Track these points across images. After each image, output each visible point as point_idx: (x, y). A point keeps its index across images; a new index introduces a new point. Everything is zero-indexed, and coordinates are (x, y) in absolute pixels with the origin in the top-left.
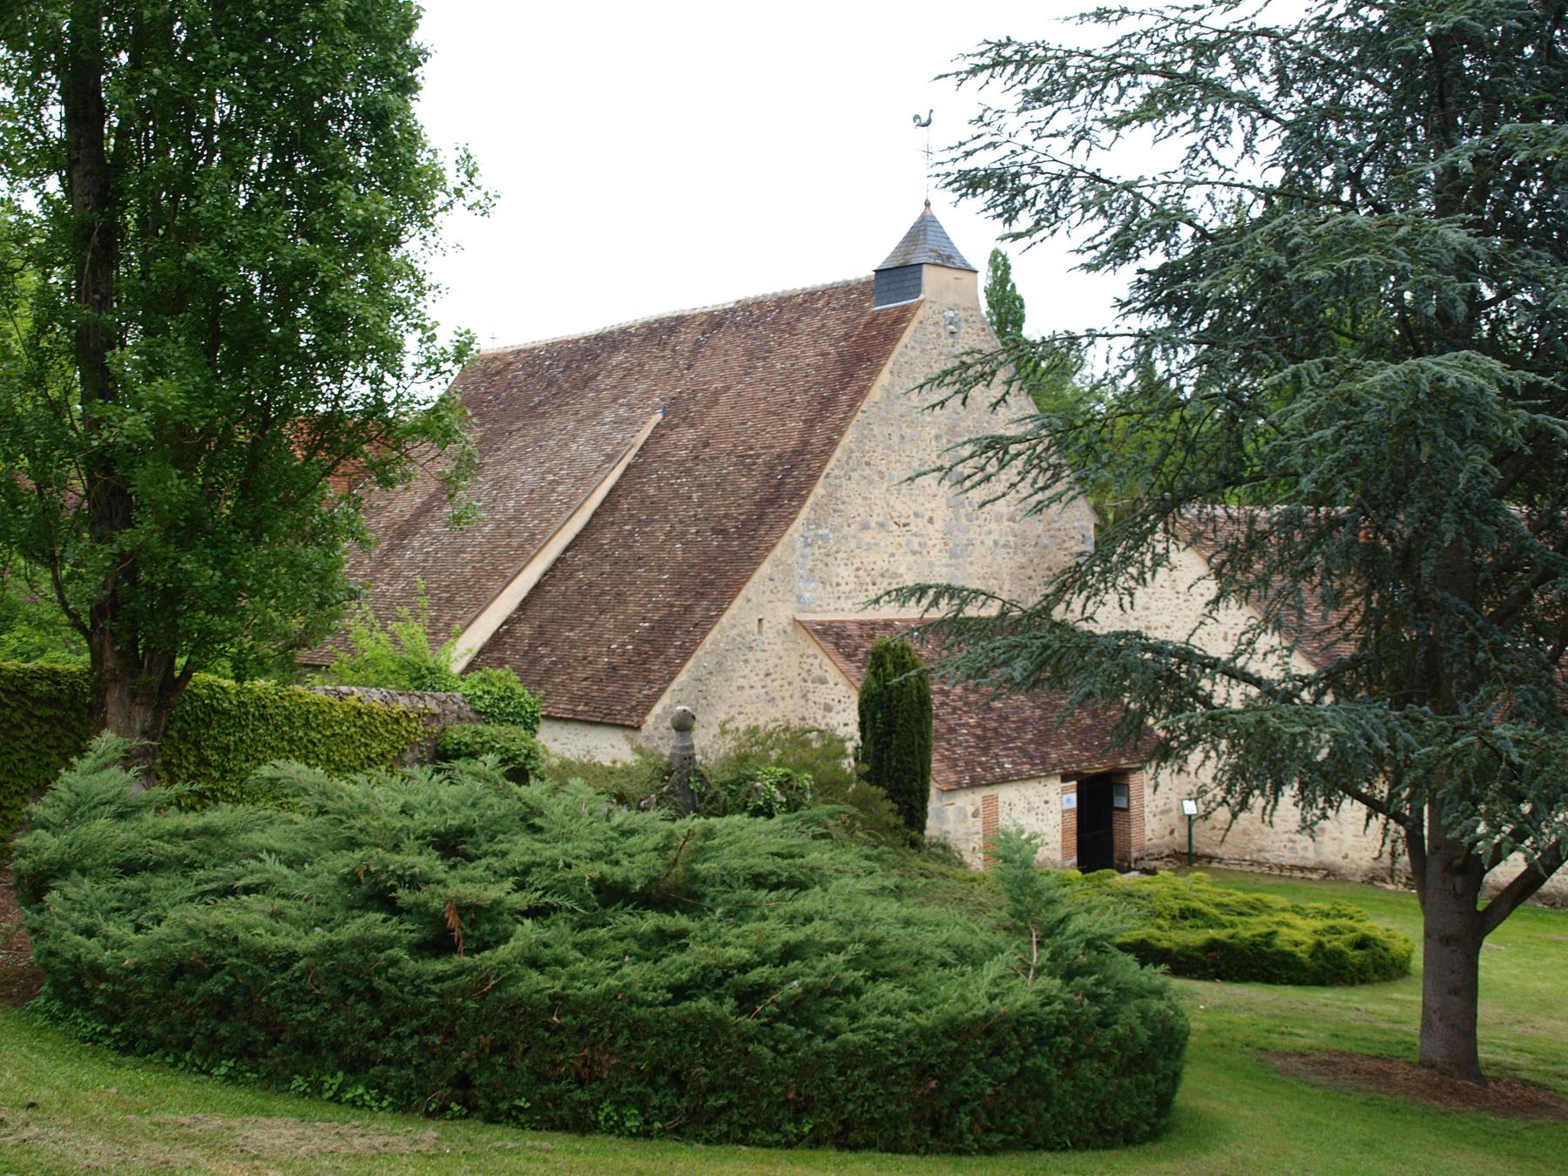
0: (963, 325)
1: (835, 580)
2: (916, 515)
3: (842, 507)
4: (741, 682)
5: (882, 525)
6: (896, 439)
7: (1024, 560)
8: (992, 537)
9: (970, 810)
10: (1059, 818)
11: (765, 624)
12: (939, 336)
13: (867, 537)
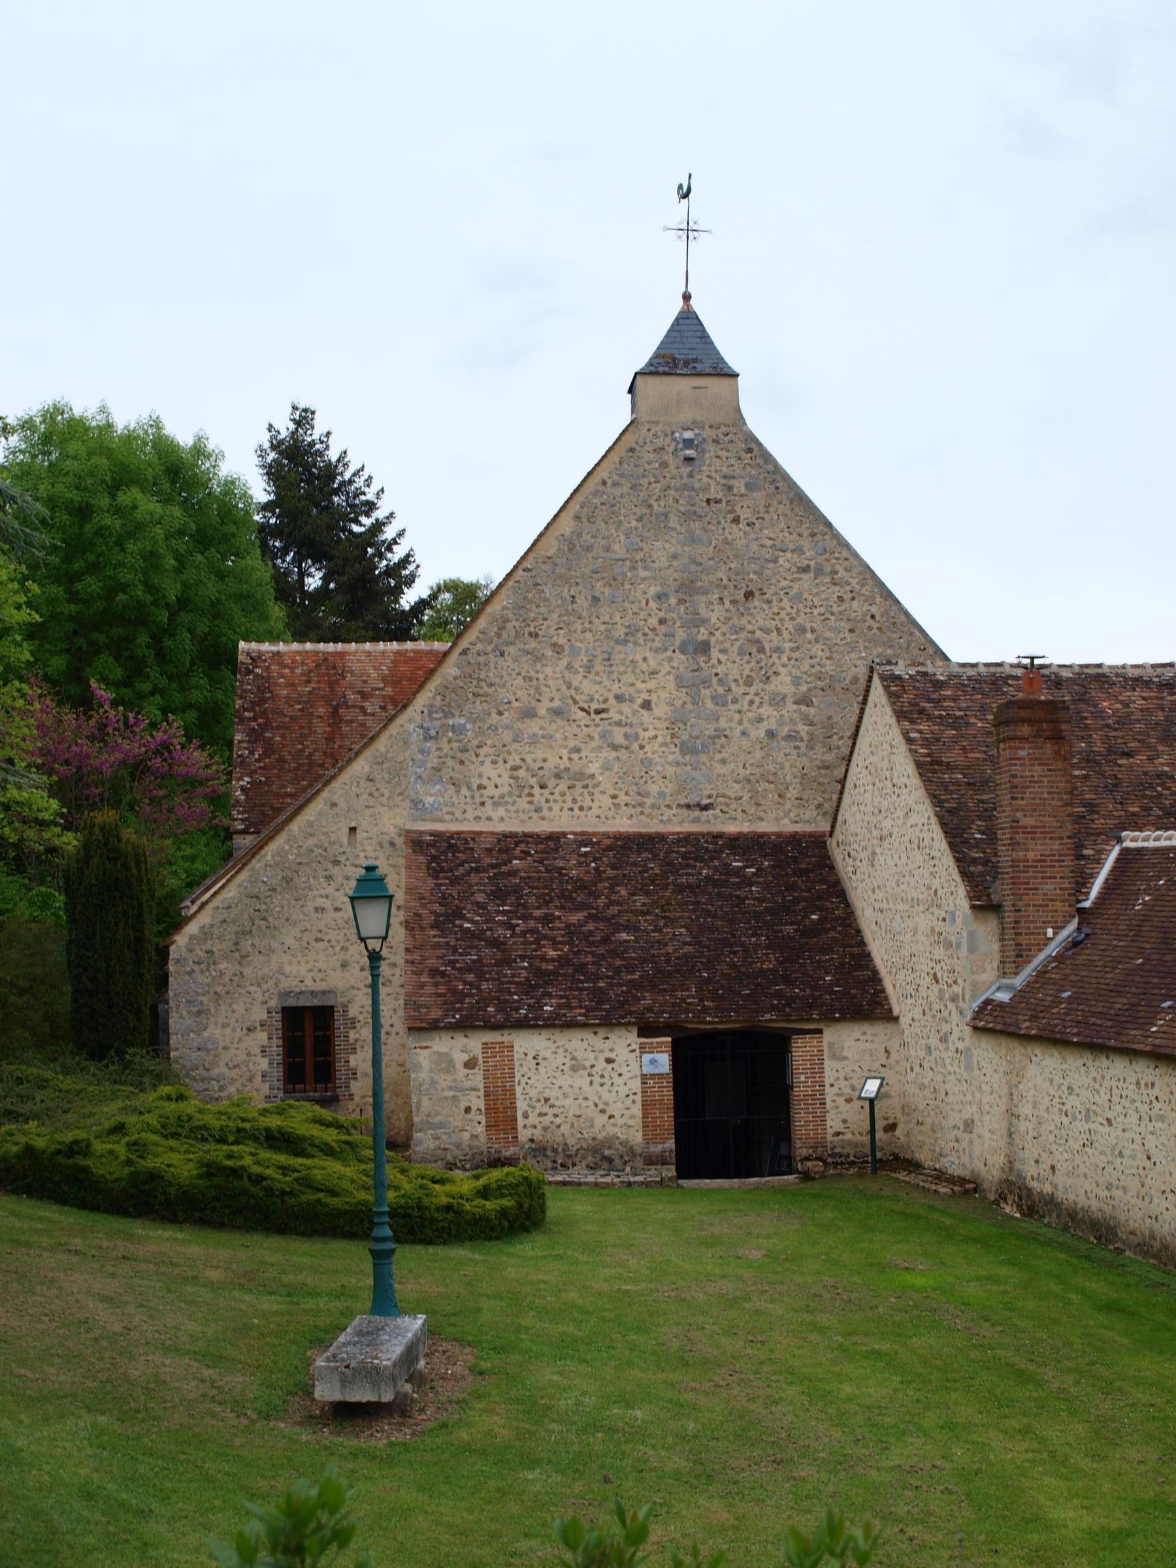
0: (711, 448)
1: (475, 782)
2: (619, 698)
3: (490, 690)
4: (320, 902)
5: (557, 713)
6: (583, 602)
7: (829, 757)
8: (764, 726)
9: (460, 1058)
10: (636, 1085)
11: (360, 835)
12: (664, 465)
13: (533, 727)
